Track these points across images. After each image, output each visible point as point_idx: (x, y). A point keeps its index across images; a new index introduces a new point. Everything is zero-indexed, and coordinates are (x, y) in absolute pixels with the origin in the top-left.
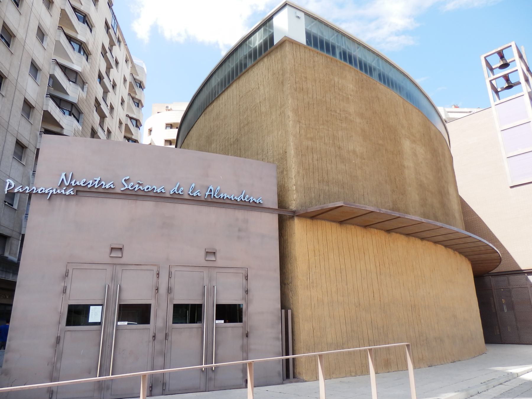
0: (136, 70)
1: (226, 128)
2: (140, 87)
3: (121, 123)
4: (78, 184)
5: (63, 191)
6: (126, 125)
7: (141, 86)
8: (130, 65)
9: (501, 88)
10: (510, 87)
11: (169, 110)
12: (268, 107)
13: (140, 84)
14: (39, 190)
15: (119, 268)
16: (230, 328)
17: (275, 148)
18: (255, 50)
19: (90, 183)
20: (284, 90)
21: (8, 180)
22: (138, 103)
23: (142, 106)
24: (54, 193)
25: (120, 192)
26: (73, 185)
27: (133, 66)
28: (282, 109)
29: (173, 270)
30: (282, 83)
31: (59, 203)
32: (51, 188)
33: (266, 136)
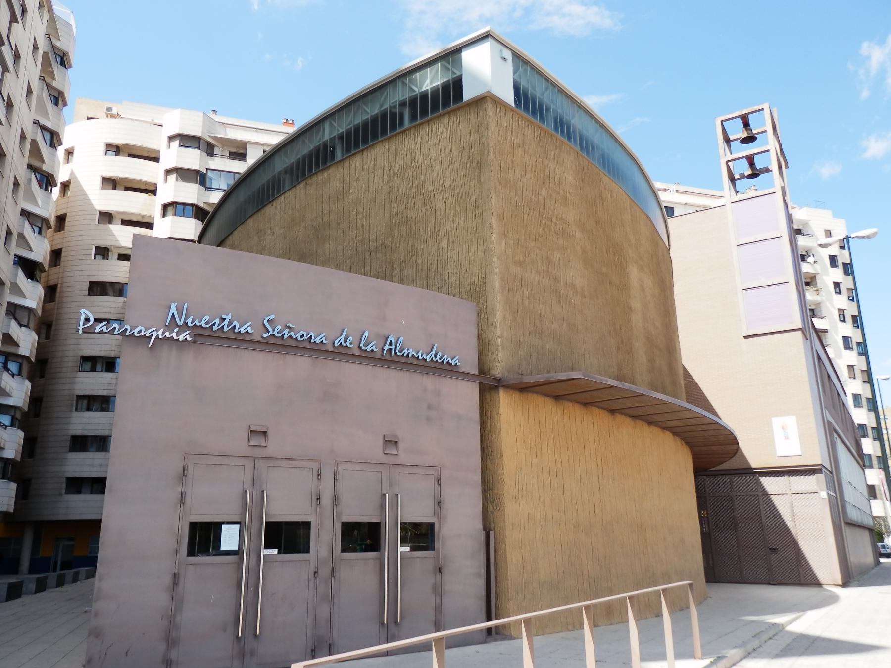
0: (56, 29)
1: (359, 221)
2: (63, 64)
3: (23, 137)
4: (198, 324)
5: (174, 335)
6: (34, 142)
7: (64, 60)
8: (46, 17)
9: (740, 174)
10: (754, 175)
11: (113, 116)
12: (450, 201)
13: (62, 59)
14: (136, 331)
15: (261, 464)
16: (418, 559)
17: (463, 272)
18: (424, 95)
19: (215, 323)
20: (482, 179)
21: (82, 311)
22: (58, 98)
23: (65, 105)
24: (160, 337)
25: (260, 339)
26: (190, 324)
27: (52, 20)
28: (478, 211)
29: (340, 468)
30: (479, 166)
31: (168, 355)
32: (155, 328)
33: (446, 250)
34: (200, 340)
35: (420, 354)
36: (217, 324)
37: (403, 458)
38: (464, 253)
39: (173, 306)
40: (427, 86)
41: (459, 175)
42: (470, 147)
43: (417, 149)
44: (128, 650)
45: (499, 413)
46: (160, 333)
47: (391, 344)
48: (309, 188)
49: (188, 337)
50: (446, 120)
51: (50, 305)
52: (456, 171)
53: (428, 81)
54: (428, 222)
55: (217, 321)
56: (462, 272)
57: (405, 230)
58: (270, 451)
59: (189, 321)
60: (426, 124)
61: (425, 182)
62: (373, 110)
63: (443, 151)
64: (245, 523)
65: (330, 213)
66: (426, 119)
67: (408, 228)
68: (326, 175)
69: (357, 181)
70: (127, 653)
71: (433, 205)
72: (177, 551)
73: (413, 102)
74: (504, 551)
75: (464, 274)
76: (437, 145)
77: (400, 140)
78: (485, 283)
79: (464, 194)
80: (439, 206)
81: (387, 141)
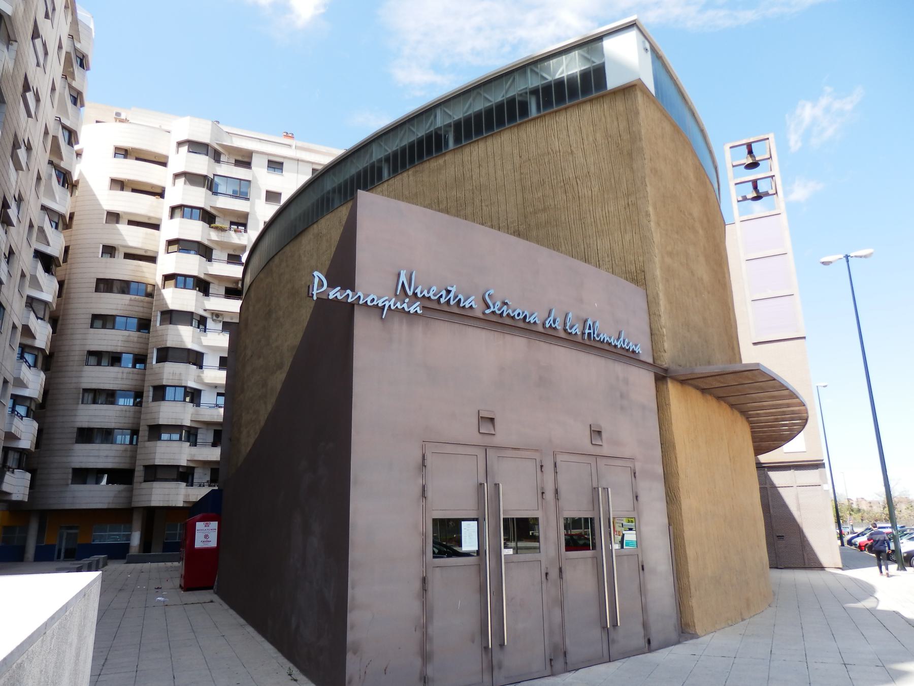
0: (78, 30)
1: (484, 208)
2: (82, 65)
3: (46, 133)
4: (427, 295)
5: (405, 306)
6: (55, 138)
7: (83, 62)
8: (70, 19)
9: (742, 197)
10: (758, 198)
11: (122, 121)
12: (596, 189)
13: (82, 60)
14: (369, 299)
16: (625, 557)
17: (616, 260)
18: (560, 83)
19: (442, 295)
20: (635, 166)
21: (316, 273)
22: (77, 98)
23: (82, 105)
24: (393, 308)
25: (481, 316)
26: (419, 295)
27: (75, 22)
28: (632, 199)
29: (560, 458)
30: (630, 154)
31: (399, 328)
32: (387, 298)
33: (595, 238)
34: (428, 314)
35: (612, 340)
36: (444, 296)
37: (606, 450)
38: (616, 241)
39: (403, 273)
40: (562, 73)
41: (606, 162)
42: (619, 135)
43: (554, 136)
44: (386, 668)
45: (669, 405)
46: (392, 303)
47: (590, 329)
48: (421, 175)
49: (418, 309)
50: (588, 107)
51: (190, 281)
52: (602, 159)
53: (564, 66)
54: (571, 209)
55: (444, 293)
56: (615, 260)
57: (543, 217)
58: (498, 440)
59: (418, 291)
60: (564, 112)
61: (565, 170)
62: (497, 96)
63: (585, 138)
64: (485, 520)
65: (449, 201)
66: (563, 106)
67: (546, 215)
68: (441, 161)
69: (481, 168)
70: (385, 670)
71: (576, 192)
72: (424, 553)
73: (547, 88)
74: (682, 547)
75: (617, 262)
76: (578, 133)
77: (532, 126)
78: (644, 271)
79: (613, 182)
80: (583, 193)
81: (516, 128)
